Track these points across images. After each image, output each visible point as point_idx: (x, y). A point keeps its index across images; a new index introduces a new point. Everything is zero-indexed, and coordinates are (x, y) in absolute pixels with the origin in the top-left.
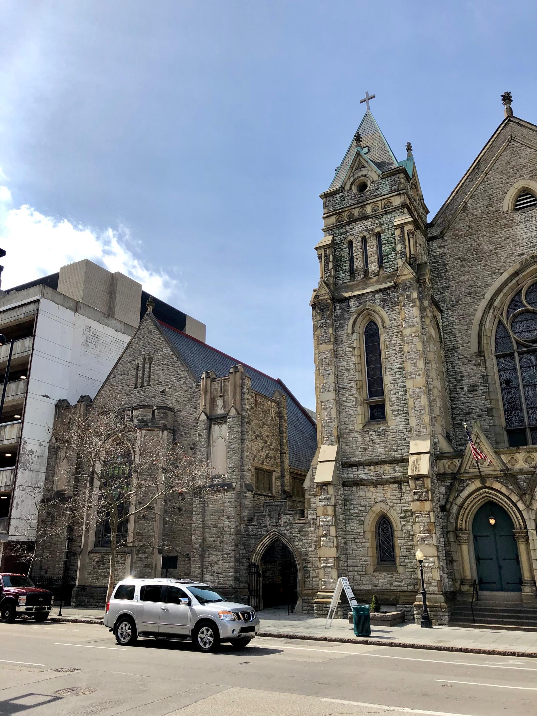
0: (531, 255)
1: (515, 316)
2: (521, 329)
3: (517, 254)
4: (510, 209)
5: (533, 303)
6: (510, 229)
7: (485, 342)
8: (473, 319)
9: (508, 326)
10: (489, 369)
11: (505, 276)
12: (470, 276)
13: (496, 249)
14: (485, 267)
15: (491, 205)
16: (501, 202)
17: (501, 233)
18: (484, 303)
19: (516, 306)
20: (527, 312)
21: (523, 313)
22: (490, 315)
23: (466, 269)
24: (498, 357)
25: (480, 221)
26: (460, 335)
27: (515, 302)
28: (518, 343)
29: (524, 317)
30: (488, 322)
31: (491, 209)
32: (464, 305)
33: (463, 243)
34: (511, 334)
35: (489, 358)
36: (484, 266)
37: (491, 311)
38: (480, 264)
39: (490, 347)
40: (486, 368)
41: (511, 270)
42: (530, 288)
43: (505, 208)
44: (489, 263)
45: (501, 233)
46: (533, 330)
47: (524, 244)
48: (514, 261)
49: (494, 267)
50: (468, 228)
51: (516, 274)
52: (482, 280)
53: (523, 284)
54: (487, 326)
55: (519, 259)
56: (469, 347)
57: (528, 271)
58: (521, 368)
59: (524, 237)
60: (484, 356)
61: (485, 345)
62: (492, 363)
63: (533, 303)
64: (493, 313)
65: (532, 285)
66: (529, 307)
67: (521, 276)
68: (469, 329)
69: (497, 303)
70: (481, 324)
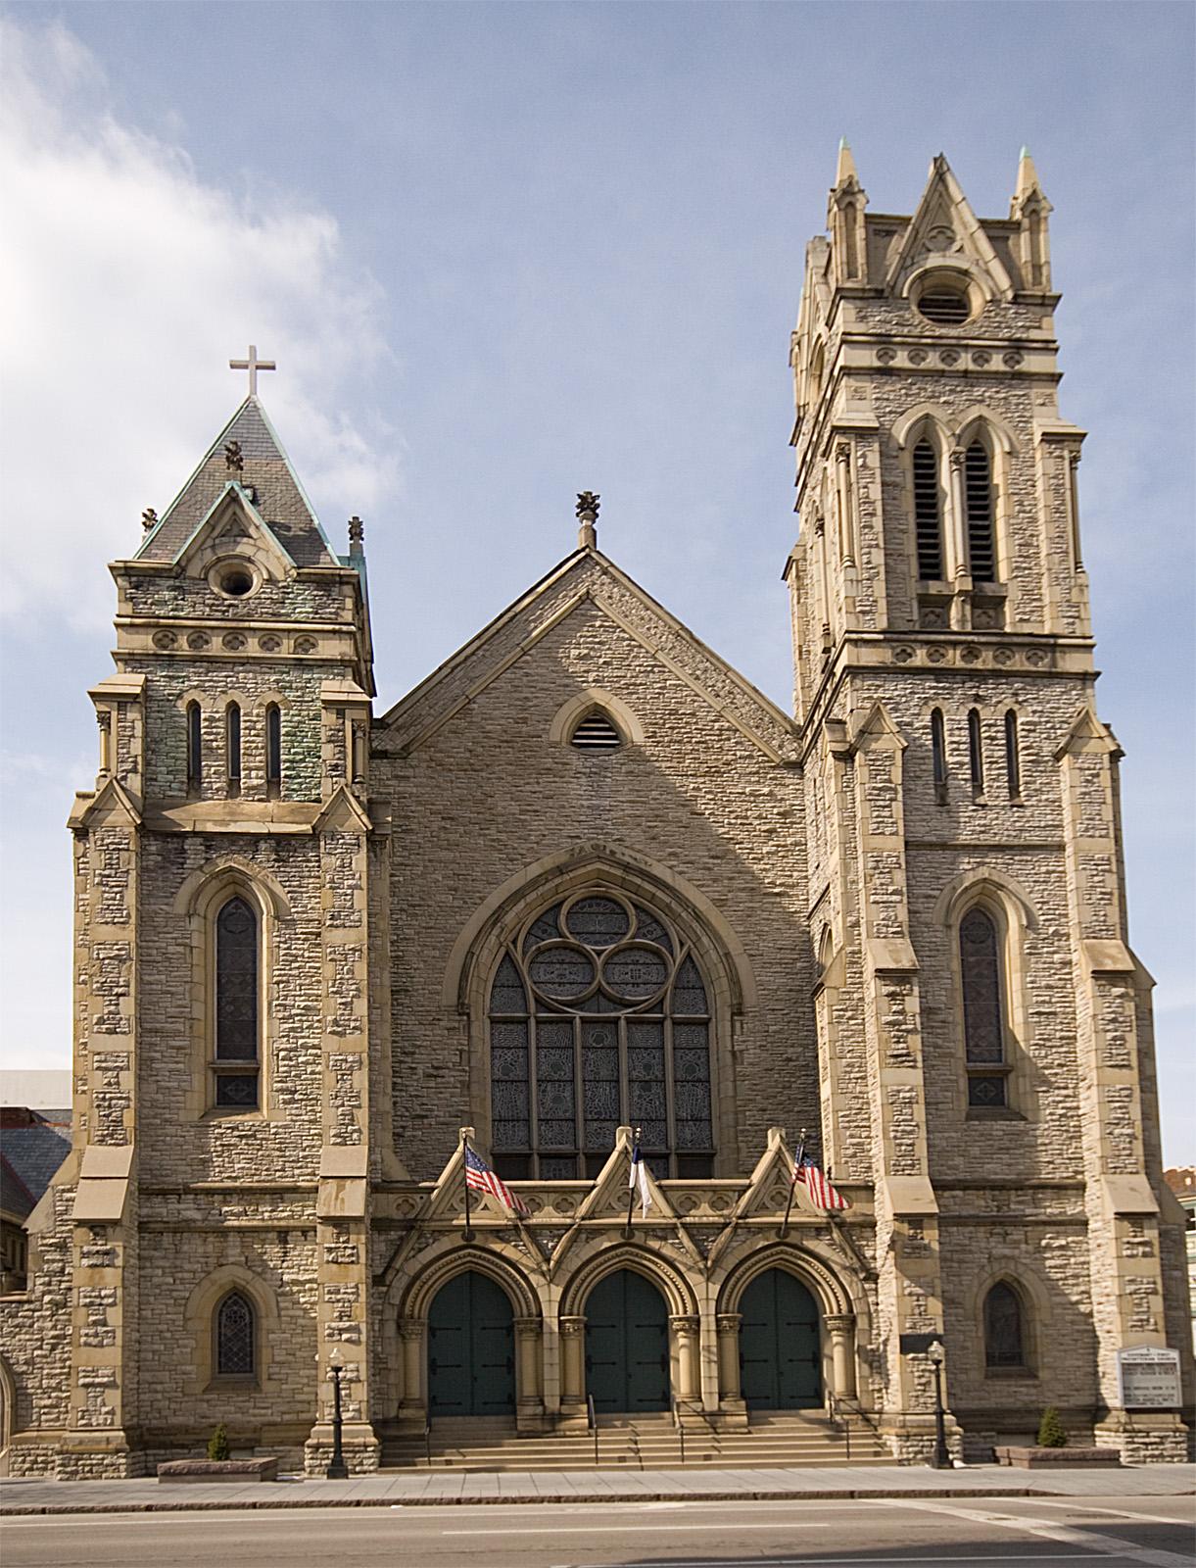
0: (592, 842)
1: (540, 952)
2: (548, 976)
3: (565, 833)
4: (564, 740)
5: (578, 933)
6: (557, 779)
7: (474, 988)
8: (454, 941)
9: (524, 969)
10: (474, 1040)
11: (535, 870)
12: (457, 854)
13: (522, 812)
14: (495, 844)
15: (525, 721)
16: (547, 721)
17: (538, 783)
18: (483, 913)
19: (545, 931)
20: (565, 948)
21: (557, 948)
22: (493, 938)
23: (453, 837)
24: (494, 1021)
25: (495, 747)
26: (422, 966)
27: (546, 922)
28: (538, 1000)
29: (555, 956)
30: (485, 952)
31: (525, 729)
32: (438, 909)
33: (452, 782)
34: (529, 982)
35: (477, 1019)
36: (493, 840)
37: (496, 931)
38: (485, 835)
39: (481, 999)
40: (470, 1037)
41: (548, 862)
42: (577, 903)
43: (555, 736)
44: (503, 837)
45: (538, 783)
46: (571, 983)
47: (583, 818)
48: (557, 845)
49: (514, 849)
50: (468, 755)
51: (560, 870)
52: (484, 869)
53: (567, 893)
54: (482, 960)
55: (567, 844)
56: (438, 993)
57: (582, 871)
58: (538, 1048)
59: (585, 803)
60: (468, 1015)
61: (473, 994)
62: (481, 1029)
63: (578, 933)
64: (498, 937)
65: (583, 900)
66: (572, 940)
67: (566, 877)
68: (444, 959)
69: (510, 918)
70: (470, 953)
